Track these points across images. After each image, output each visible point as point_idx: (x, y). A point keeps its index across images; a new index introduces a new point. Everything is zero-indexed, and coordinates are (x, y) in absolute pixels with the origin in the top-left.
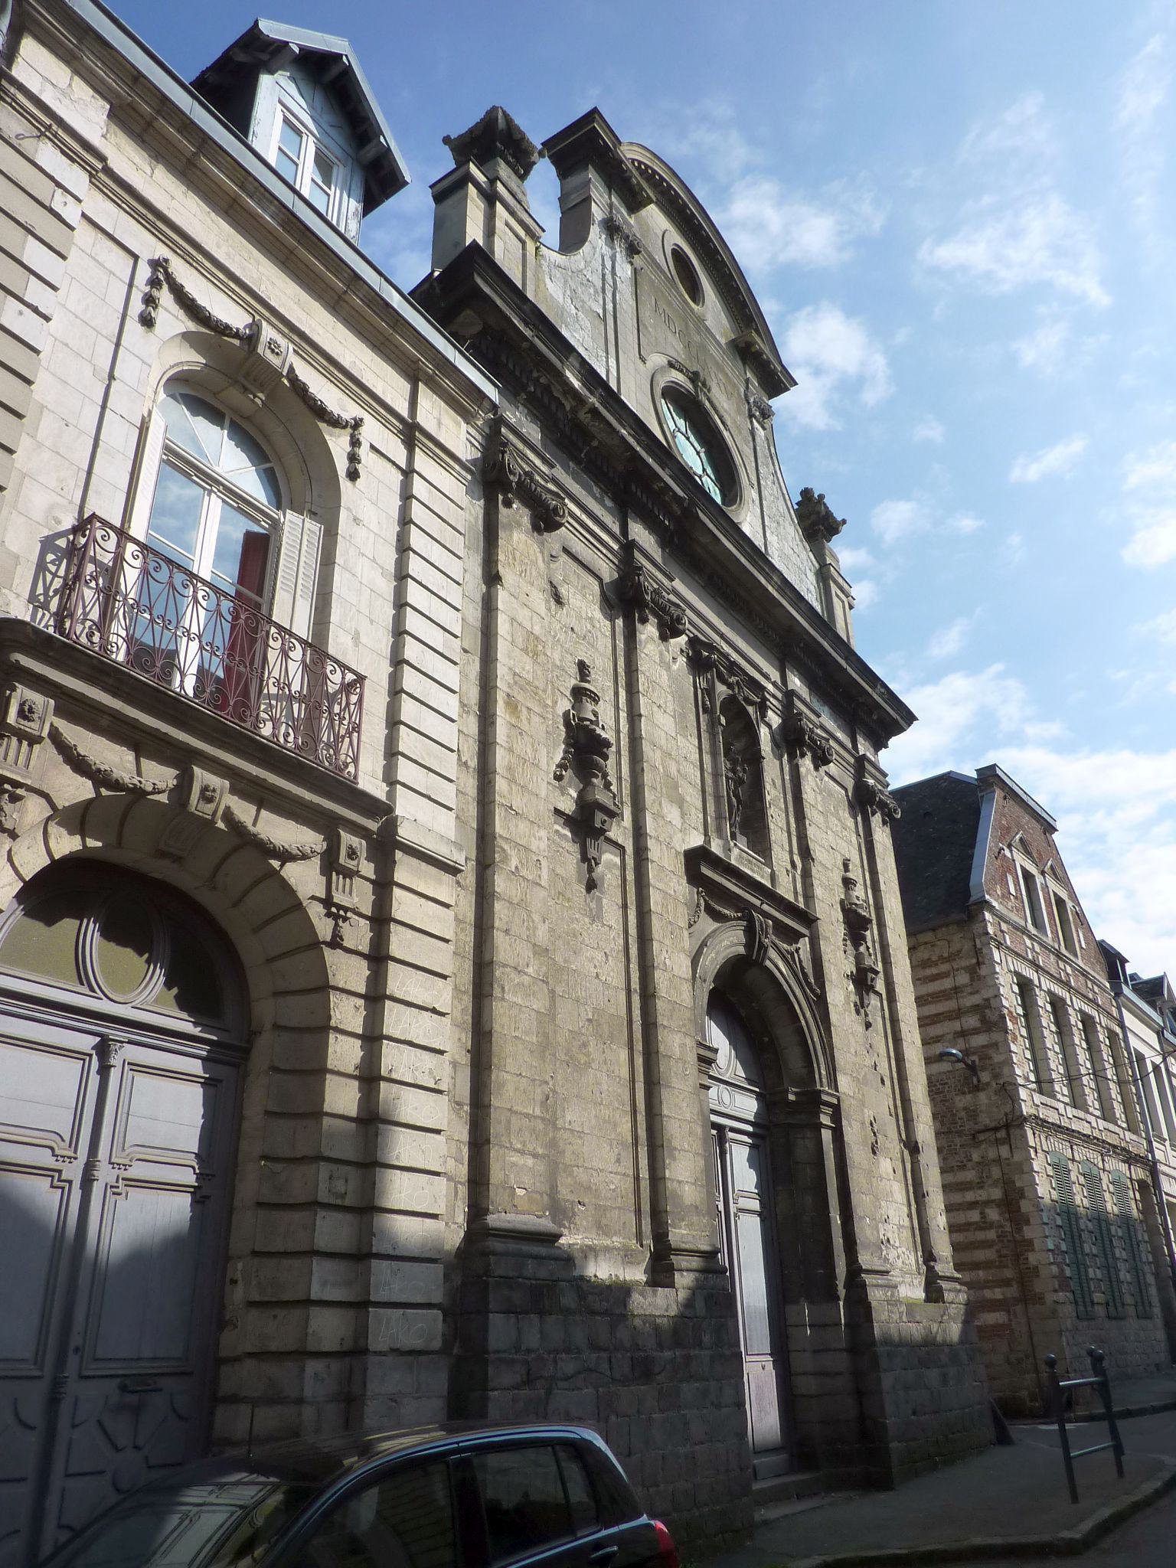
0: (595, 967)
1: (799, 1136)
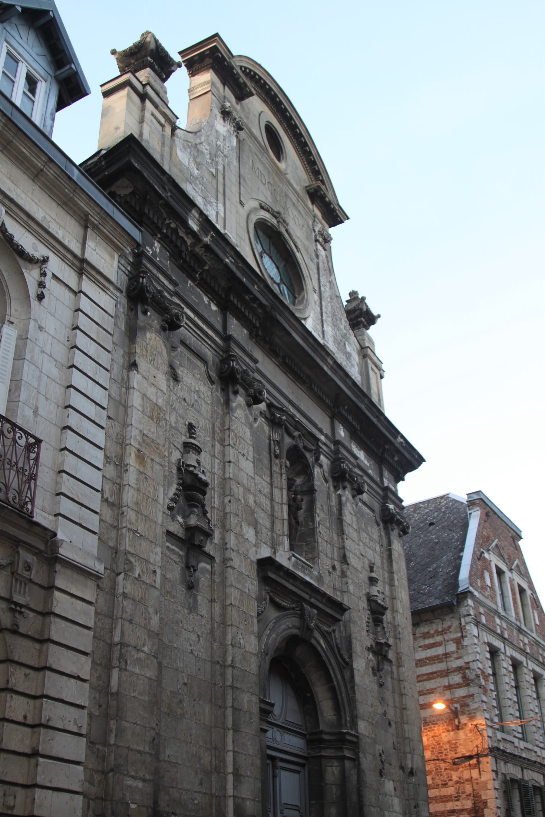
0: (191, 645)
1: (329, 765)
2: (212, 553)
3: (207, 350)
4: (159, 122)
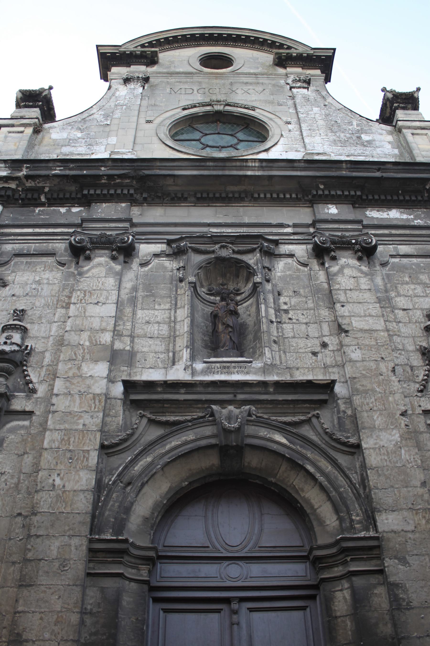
1: (337, 589)
2: (27, 409)
3: (57, 245)
4: (19, 132)
